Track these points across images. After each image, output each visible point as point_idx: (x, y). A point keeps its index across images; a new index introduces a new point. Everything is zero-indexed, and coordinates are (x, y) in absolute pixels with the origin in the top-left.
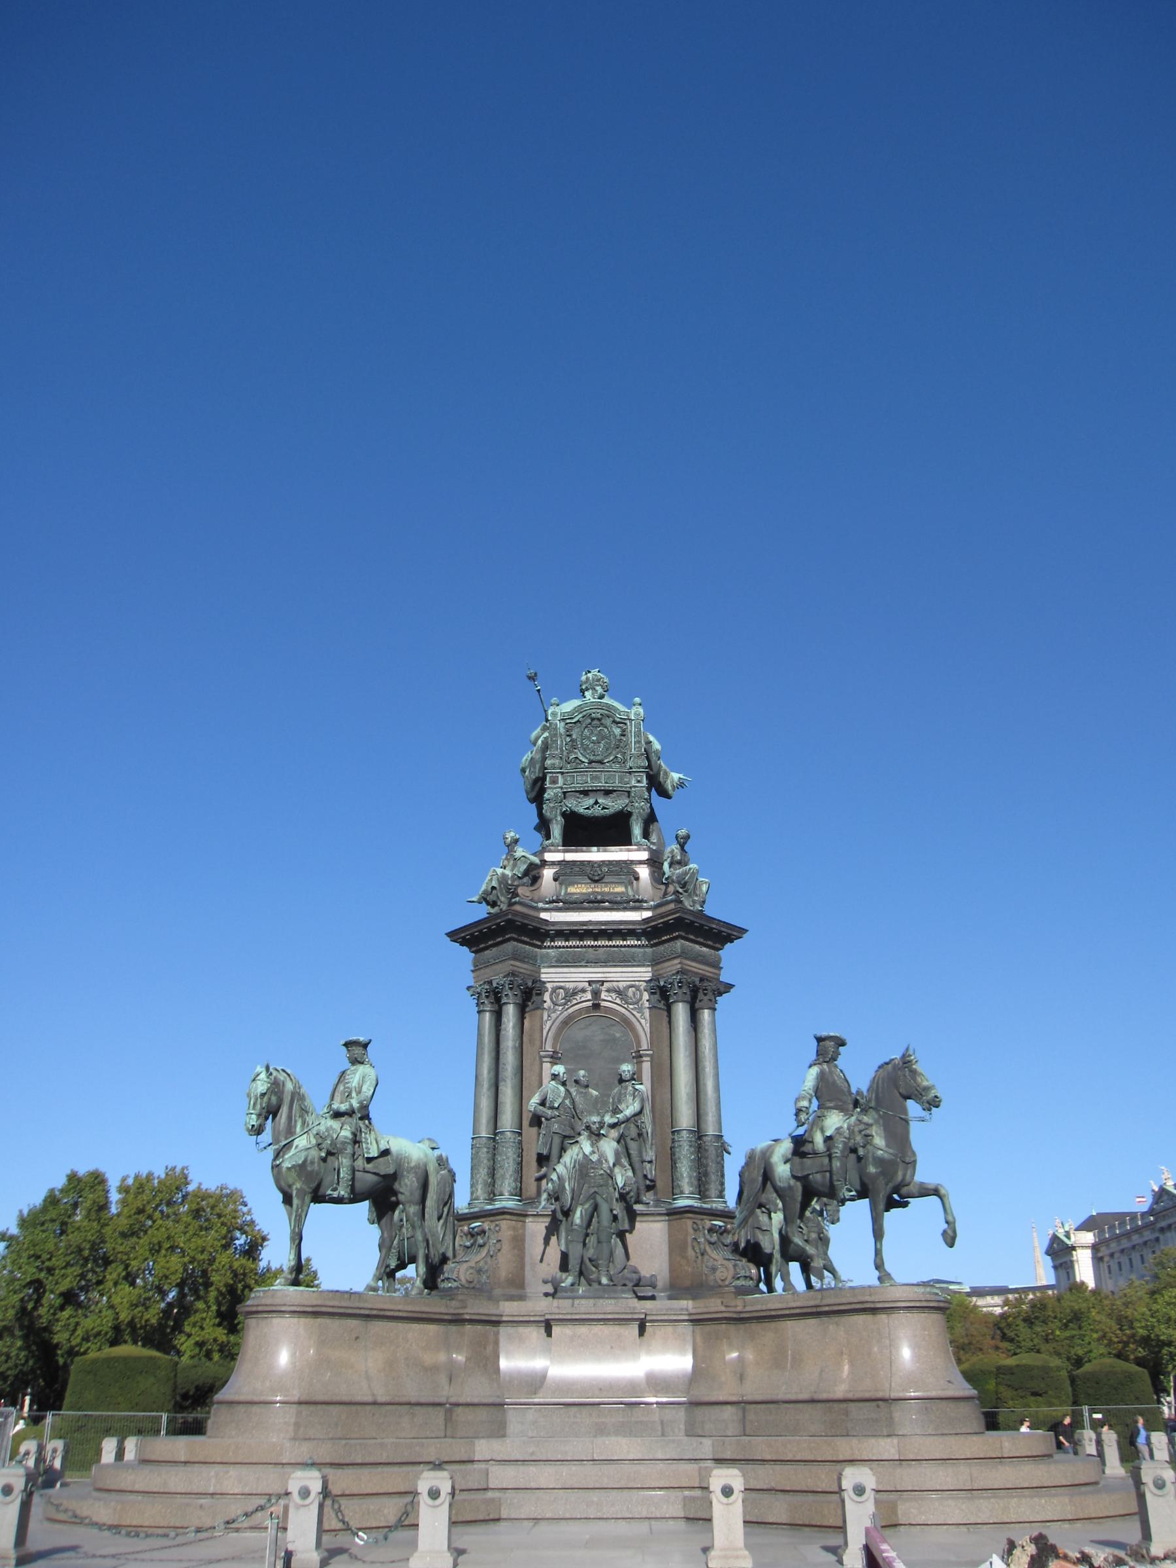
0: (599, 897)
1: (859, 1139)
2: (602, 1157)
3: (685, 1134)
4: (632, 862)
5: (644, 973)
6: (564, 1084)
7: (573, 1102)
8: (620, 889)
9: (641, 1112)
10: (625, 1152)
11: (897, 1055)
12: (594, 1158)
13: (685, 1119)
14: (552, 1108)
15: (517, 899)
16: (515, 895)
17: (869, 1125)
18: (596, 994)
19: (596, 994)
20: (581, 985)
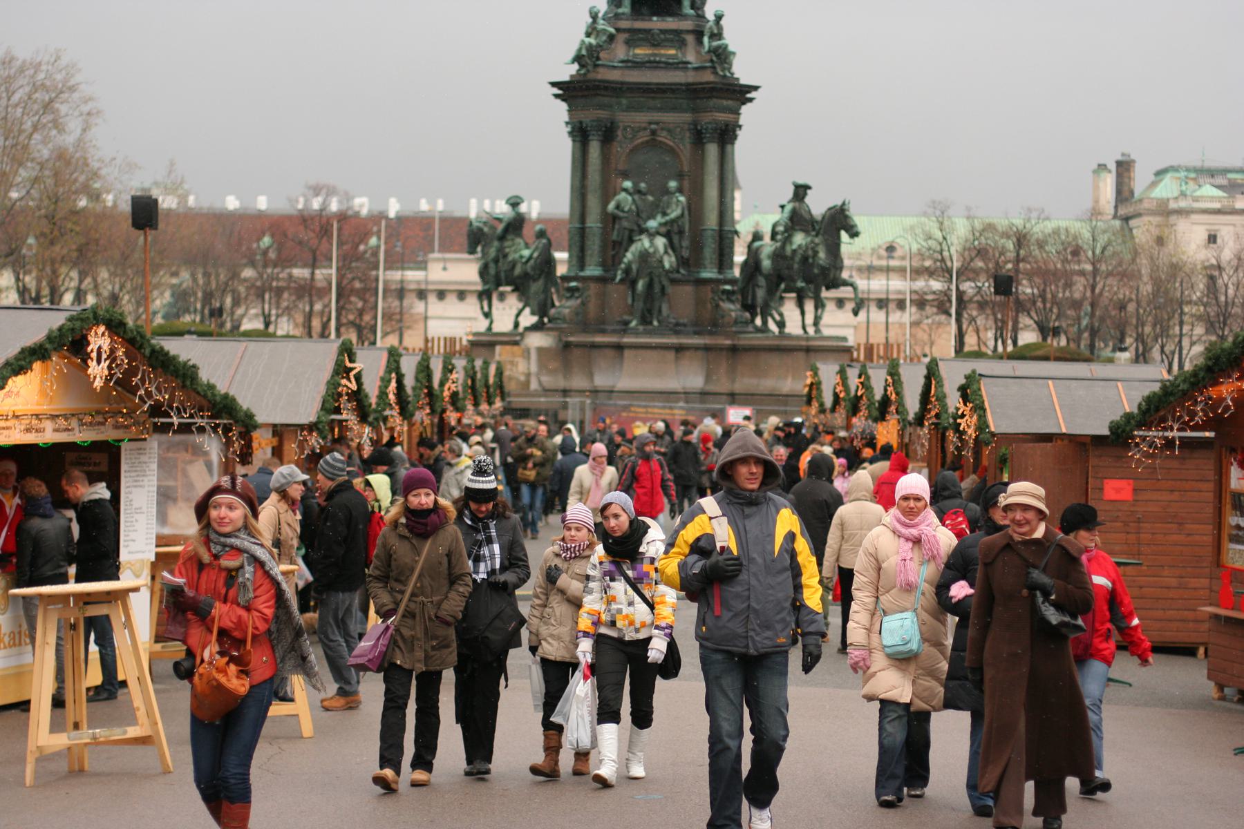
0: (658, 59)
1: (810, 253)
2: (656, 251)
3: (709, 233)
4: (682, 32)
5: (687, 117)
6: (630, 194)
7: (637, 207)
8: (672, 52)
9: (682, 215)
10: (671, 245)
11: (839, 203)
12: (651, 250)
13: (711, 221)
14: (623, 211)
15: (600, 62)
16: (598, 58)
17: (817, 245)
18: (653, 133)
19: (653, 133)
20: (644, 125)
